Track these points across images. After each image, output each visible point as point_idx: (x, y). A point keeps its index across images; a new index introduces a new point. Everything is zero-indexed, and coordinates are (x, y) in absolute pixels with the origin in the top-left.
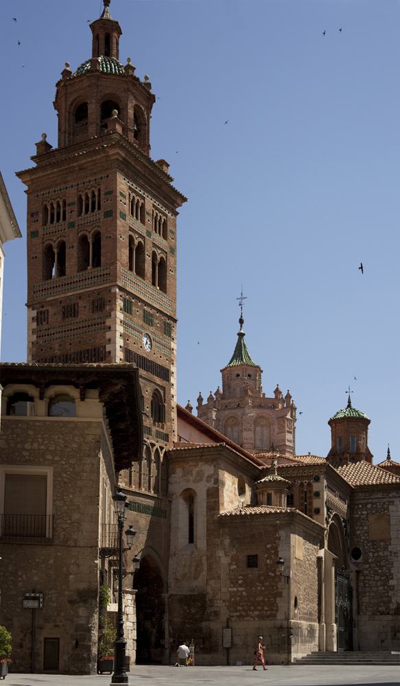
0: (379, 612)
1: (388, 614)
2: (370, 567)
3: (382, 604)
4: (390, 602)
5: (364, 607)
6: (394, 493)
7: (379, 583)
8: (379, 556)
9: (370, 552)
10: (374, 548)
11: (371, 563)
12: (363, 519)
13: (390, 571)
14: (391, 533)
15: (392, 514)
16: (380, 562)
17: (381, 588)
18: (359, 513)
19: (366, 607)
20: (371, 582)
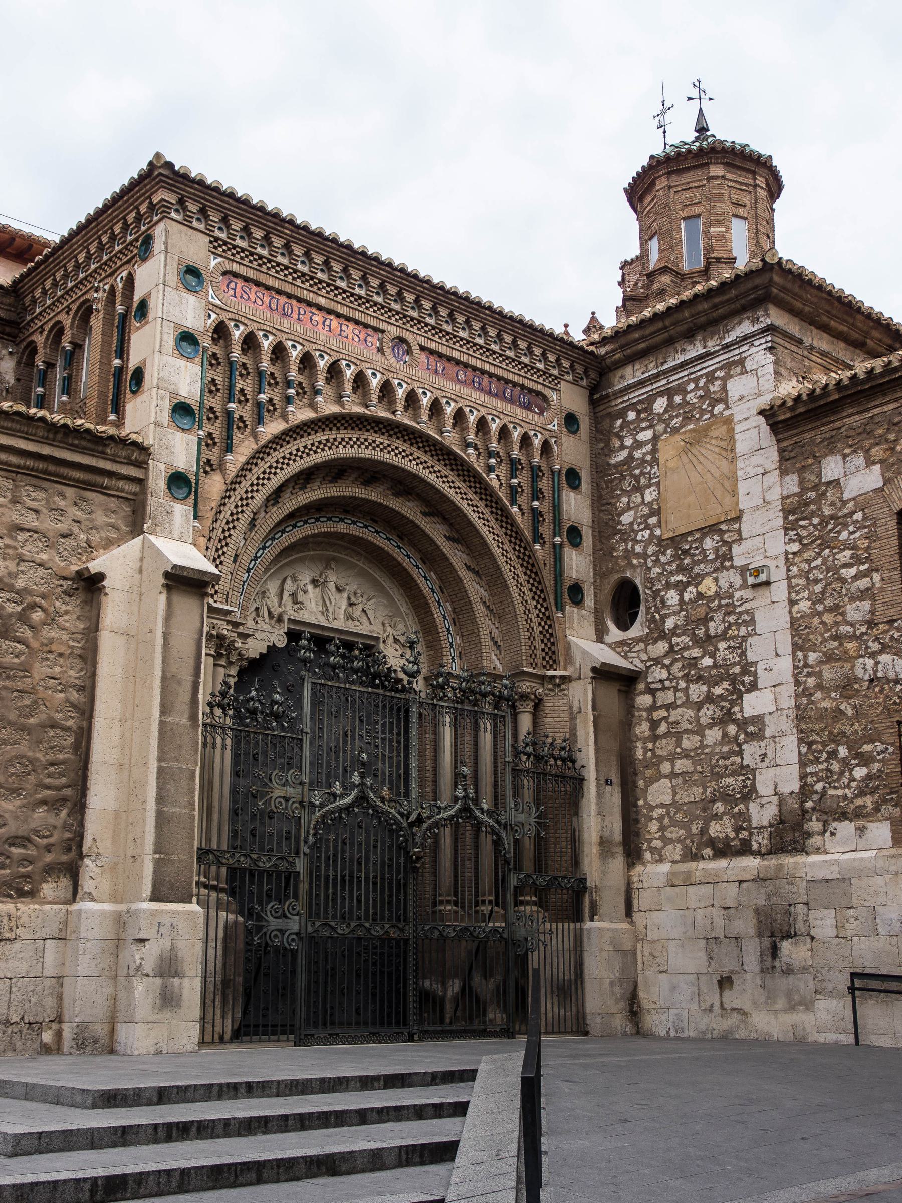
0: (711, 842)
1: (745, 849)
2: (672, 646)
3: (719, 807)
4: (749, 794)
5: (654, 826)
6: (745, 328)
7: (708, 713)
8: (700, 595)
9: (668, 586)
10: (681, 569)
11: (674, 632)
12: (643, 461)
13: (744, 653)
14: (742, 488)
15: (739, 411)
16: (706, 620)
17: (713, 735)
18: (628, 442)
19: (662, 828)
20: (675, 715)
